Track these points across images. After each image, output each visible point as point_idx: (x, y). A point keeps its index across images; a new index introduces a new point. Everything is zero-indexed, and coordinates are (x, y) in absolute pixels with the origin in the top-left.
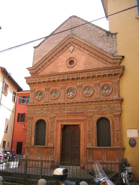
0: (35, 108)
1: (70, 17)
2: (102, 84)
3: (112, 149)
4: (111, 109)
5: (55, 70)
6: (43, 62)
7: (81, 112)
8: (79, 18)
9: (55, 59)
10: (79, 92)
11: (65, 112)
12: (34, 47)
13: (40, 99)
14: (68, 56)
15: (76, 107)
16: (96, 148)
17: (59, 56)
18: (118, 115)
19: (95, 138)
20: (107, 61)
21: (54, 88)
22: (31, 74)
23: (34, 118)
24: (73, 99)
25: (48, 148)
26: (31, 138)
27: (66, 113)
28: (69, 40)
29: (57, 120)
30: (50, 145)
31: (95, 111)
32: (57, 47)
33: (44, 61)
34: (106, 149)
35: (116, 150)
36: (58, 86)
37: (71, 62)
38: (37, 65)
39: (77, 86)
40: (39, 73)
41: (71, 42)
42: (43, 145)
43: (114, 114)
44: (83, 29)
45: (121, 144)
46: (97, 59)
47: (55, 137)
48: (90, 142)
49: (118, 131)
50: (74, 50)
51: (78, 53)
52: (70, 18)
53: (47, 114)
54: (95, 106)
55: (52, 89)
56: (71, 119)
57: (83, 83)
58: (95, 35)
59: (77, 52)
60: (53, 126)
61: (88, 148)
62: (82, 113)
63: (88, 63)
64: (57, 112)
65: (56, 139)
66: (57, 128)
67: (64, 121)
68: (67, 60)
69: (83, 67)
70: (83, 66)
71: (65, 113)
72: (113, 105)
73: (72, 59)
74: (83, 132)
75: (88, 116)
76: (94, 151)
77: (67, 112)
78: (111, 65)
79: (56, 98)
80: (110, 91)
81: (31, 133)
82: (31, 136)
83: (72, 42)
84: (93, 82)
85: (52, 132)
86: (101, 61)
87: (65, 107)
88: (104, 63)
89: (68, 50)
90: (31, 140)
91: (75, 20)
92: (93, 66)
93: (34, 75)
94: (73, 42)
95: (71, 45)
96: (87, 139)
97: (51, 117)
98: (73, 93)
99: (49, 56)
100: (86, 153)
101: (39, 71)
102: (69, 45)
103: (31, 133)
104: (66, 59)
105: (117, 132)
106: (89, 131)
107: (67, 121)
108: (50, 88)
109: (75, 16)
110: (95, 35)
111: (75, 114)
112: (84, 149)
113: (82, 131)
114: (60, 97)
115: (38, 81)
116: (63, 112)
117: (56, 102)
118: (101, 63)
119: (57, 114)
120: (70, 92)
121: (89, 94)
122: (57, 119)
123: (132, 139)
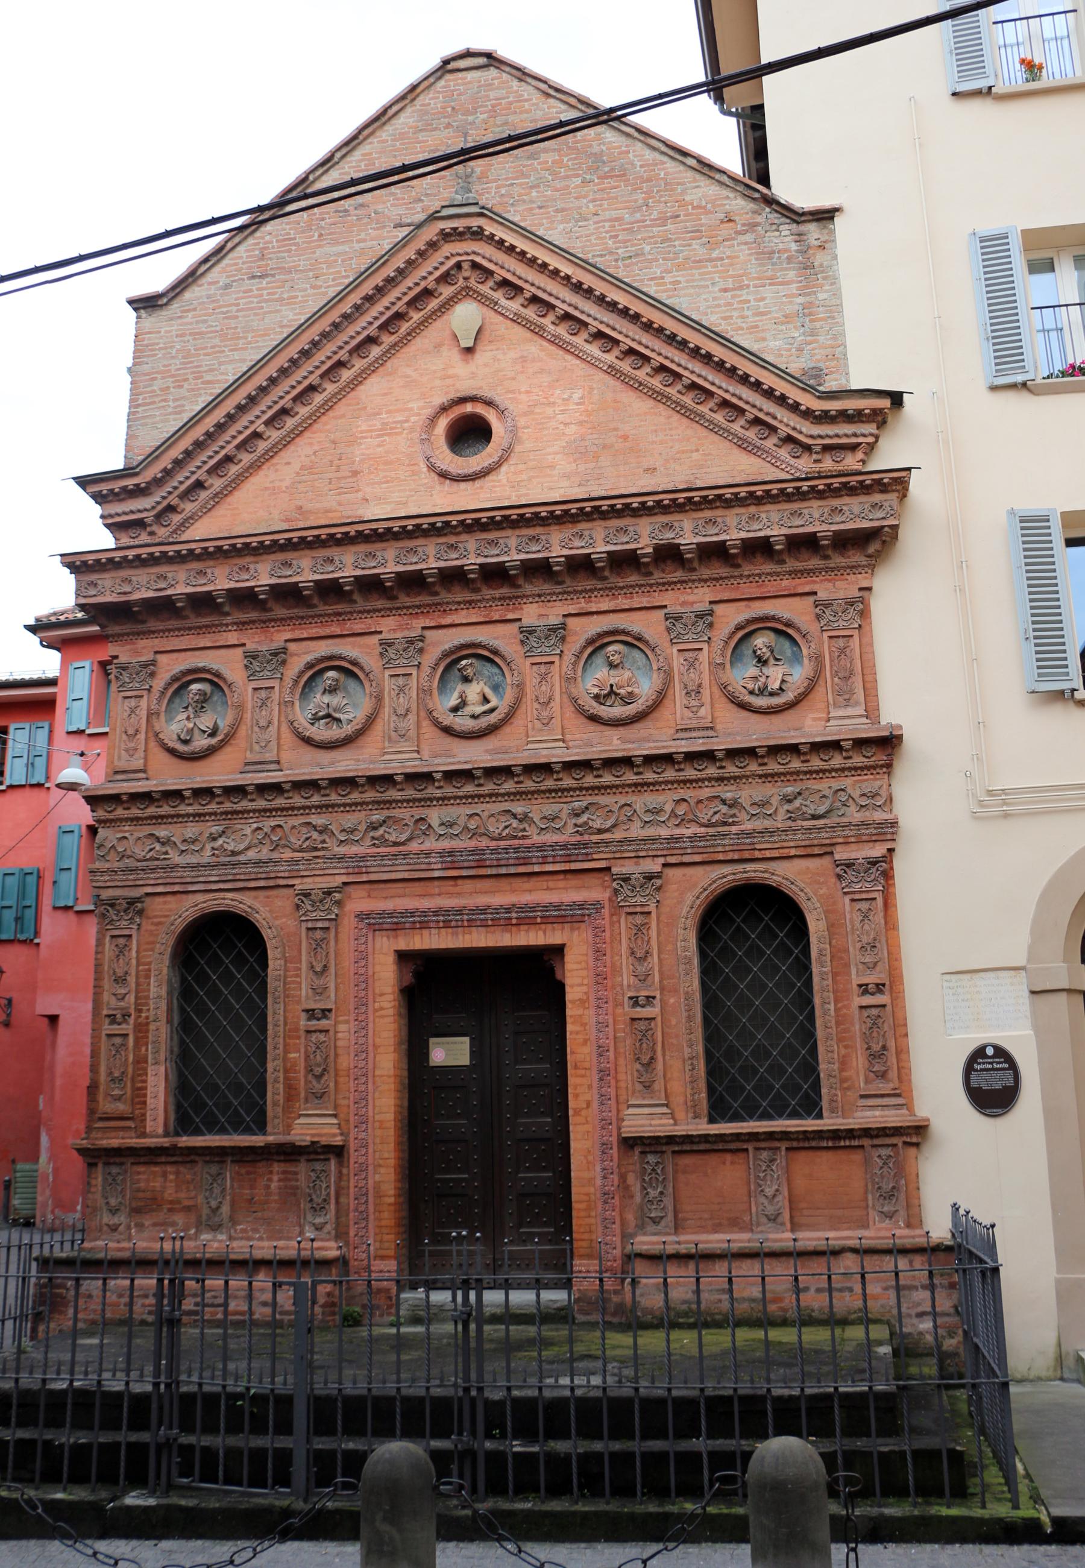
0: (159, 819)
1: (446, 62)
2: (731, 616)
4: (814, 817)
5: (330, 501)
6: (220, 427)
7: (565, 847)
8: (522, 74)
9: (327, 407)
10: (543, 677)
11: (430, 844)
12: (131, 302)
13: (201, 742)
14: (438, 382)
15: (518, 808)
16: (705, 1138)
18: (873, 863)
19: (687, 1051)
21: (323, 649)
22: (115, 527)
23: (156, 906)
24: (490, 743)
25: (289, 1153)
27: (441, 853)
28: (447, 249)
29: (361, 916)
31: (688, 832)
32: (346, 307)
33: (231, 418)
34: (785, 1136)
35: (866, 1142)
36: (358, 627)
38: (176, 452)
39: (528, 632)
40: (183, 525)
41: (458, 266)
42: (248, 1131)
43: (841, 854)
44: (559, 163)
47: (345, 1061)
48: (648, 1086)
49: (879, 988)
50: (486, 333)
51: (523, 359)
52: (446, 66)
54: (683, 793)
55: (309, 658)
56: (482, 900)
57: (572, 609)
58: (663, 220)
59: (512, 354)
60: (325, 967)
61: (629, 1143)
63: (605, 447)
64: (354, 849)
65: (364, 1075)
66: (364, 981)
67: (421, 921)
68: (433, 420)
71: (428, 854)
72: (825, 785)
73: (469, 408)
74: (592, 1012)
75: (626, 879)
76: (686, 1161)
77: (446, 844)
78: (805, 464)
79: (348, 729)
80: (799, 675)
82: (141, 1062)
83: (465, 266)
84: (658, 599)
85: (325, 1013)
86: (713, 428)
88: (743, 445)
89: (436, 331)
90: (139, 1096)
91: (489, 86)
92: (650, 470)
94: (475, 266)
95: (467, 293)
96: (622, 1069)
98: (496, 688)
99: (273, 381)
100: (623, 1177)
101: (189, 507)
102: (447, 291)
103: (141, 1029)
104: (420, 408)
105: (868, 1000)
106: (635, 1001)
107: (447, 919)
109: (491, 59)
110: (663, 220)
112: (605, 1146)
113: (582, 1002)
114: (379, 727)
116: (414, 846)
117: (343, 763)
120: (466, 680)
121: (631, 694)
122: (359, 902)
123: (990, 1051)
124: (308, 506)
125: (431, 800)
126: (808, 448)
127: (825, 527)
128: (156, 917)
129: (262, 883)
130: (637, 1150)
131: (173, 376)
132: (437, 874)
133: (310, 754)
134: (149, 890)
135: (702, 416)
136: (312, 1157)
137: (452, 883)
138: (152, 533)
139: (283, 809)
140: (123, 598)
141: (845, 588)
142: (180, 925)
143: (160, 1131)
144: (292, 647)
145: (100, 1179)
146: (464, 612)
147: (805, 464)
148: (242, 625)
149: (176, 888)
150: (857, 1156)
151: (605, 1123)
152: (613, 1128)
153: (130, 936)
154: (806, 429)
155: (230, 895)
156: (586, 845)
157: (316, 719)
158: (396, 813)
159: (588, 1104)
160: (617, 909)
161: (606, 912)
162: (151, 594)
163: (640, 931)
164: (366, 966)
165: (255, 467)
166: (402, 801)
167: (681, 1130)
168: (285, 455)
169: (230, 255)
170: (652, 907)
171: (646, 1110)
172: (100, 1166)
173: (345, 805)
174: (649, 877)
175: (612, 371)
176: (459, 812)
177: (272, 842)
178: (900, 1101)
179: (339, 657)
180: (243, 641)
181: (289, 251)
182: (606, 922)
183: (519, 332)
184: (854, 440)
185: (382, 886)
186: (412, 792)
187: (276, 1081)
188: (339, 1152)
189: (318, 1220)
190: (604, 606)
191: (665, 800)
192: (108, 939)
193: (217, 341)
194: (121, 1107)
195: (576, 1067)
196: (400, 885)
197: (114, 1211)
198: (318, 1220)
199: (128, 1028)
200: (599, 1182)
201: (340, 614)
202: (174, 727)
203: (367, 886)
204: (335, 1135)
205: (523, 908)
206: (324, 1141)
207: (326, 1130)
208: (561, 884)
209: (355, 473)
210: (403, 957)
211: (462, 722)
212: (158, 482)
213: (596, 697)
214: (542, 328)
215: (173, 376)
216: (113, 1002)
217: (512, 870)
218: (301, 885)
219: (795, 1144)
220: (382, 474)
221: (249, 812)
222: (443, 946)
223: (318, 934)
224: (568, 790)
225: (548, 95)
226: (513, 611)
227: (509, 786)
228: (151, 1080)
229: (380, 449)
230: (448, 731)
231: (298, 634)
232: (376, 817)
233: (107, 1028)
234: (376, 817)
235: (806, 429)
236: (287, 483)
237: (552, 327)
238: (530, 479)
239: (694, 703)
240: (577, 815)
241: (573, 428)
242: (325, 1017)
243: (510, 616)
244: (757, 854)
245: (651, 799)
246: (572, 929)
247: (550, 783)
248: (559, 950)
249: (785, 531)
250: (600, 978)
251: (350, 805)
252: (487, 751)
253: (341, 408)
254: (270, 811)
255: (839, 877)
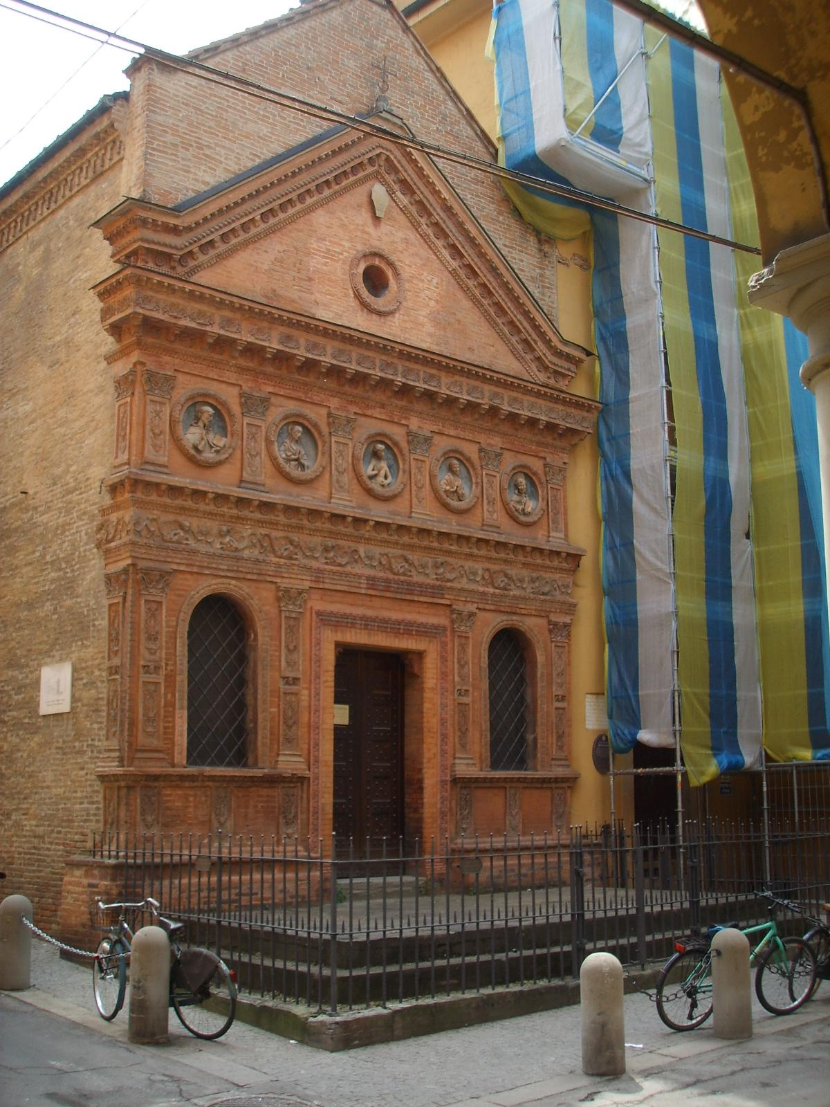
0: (183, 510)
3: (544, 781)
9: (292, 220)
11: (358, 569)
13: (209, 455)
14: (359, 234)
16: (485, 780)
17: (311, 209)
20: (533, 350)
21: (292, 407)
23: (179, 581)
25: (272, 781)
26: (170, 716)
27: (369, 578)
29: (319, 613)
30: (290, 763)
36: (316, 399)
37: (375, 280)
40: (193, 271)
41: (378, 155)
45: (567, 760)
46: (486, 315)
47: (304, 718)
48: (463, 746)
49: (563, 698)
53: (263, 566)
56: (385, 614)
61: (455, 781)
62: (438, 590)
69: (430, 335)
70: (429, 327)
71: (360, 577)
75: (460, 614)
76: (479, 793)
77: (372, 572)
78: (542, 377)
81: (170, 679)
82: (170, 705)
86: (501, 336)
87: (359, 539)
88: (513, 351)
92: (471, 349)
93: (165, 269)
97: (287, 591)
101: (202, 258)
103: (170, 679)
107: (368, 623)
108: (273, 400)
111: (404, 592)
112: (443, 782)
113: (433, 689)
115: (216, 329)
116: (348, 569)
118: (501, 347)
119: (318, 575)
122: (317, 604)
124: (280, 292)
125: (361, 538)
126: (546, 368)
127: (563, 423)
128: (178, 589)
129: (255, 577)
130: (459, 785)
131: (180, 136)
132: (363, 591)
133: (284, 485)
134: (175, 567)
135: (497, 325)
136: (287, 785)
137: (368, 599)
138: (173, 268)
139: (271, 523)
140: (173, 321)
141: (555, 460)
142: (197, 600)
143: (185, 762)
144: (273, 400)
145: (139, 800)
146: (378, 410)
147: (542, 377)
148: (242, 370)
149: (195, 570)
150: (548, 793)
151: (444, 768)
152: (448, 772)
153: (160, 603)
154: (550, 358)
155: (233, 582)
156: (441, 588)
157: (288, 460)
158: (340, 542)
159: (435, 755)
160: (453, 631)
161: (448, 633)
162: (193, 325)
163: (463, 648)
164: (319, 650)
165: (245, 244)
166: (345, 535)
167: (483, 774)
168: (264, 244)
169: (221, 56)
170: (470, 635)
171: (465, 762)
172: (138, 789)
173: (310, 530)
174: (471, 615)
175: (453, 273)
176: (377, 551)
177: (262, 546)
178: (565, 763)
179: (304, 417)
180: (240, 383)
181: (263, 76)
182: (449, 639)
183: (402, 219)
184: (567, 373)
185: (329, 593)
186: (353, 531)
187: (265, 728)
188: (302, 780)
189: (290, 831)
190: (452, 432)
191: (479, 567)
192: (143, 602)
193: (212, 124)
194: (155, 743)
195: (429, 731)
196: (340, 594)
197: (148, 826)
198: (290, 831)
199: (161, 678)
200: (439, 806)
201: (306, 384)
202: (192, 436)
203: (320, 591)
204: (304, 770)
205: (410, 624)
206: (299, 773)
207: (299, 766)
208: (426, 611)
209: (310, 279)
210: (337, 644)
211: (374, 485)
212: (189, 229)
213: (446, 491)
214: (419, 225)
215: (180, 136)
216: (148, 656)
217: (403, 597)
218: (284, 583)
219: (526, 785)
220: (327, 288)
221: (247, 520)
222: (362, 642)
223: (292, 622)
224: (434, 549)
225: (420, 55)
226: (406, 418)
227: (405, 539)
228: (178, 721)
229: (325, 268)
230: (369, 492)
231: (276, 390)
232: (330, 543)
233: (143, 677)
234: (441, 559)
235: (550, 358)
236: (265, 267)
237: (425, 227)
238: (412, 328)
239: (491, 509)
240: (437, 568)
241: (432, 303)
242: (294, 684)
243: (403, 422)
244: (518, 610)
245: (468, 564)
246: (430, 642)
247: (426, 543)
248: (420, 655)
249: (547, 419)
250: (444, 676)
251: (314, 530)
252: (389, 512)
253: (301, 224)
254: (262, 522)
255: (550, 631)
